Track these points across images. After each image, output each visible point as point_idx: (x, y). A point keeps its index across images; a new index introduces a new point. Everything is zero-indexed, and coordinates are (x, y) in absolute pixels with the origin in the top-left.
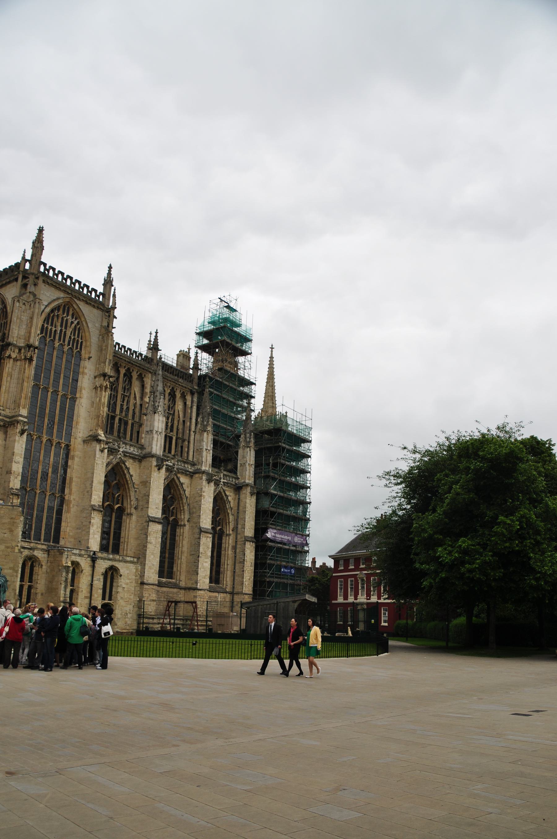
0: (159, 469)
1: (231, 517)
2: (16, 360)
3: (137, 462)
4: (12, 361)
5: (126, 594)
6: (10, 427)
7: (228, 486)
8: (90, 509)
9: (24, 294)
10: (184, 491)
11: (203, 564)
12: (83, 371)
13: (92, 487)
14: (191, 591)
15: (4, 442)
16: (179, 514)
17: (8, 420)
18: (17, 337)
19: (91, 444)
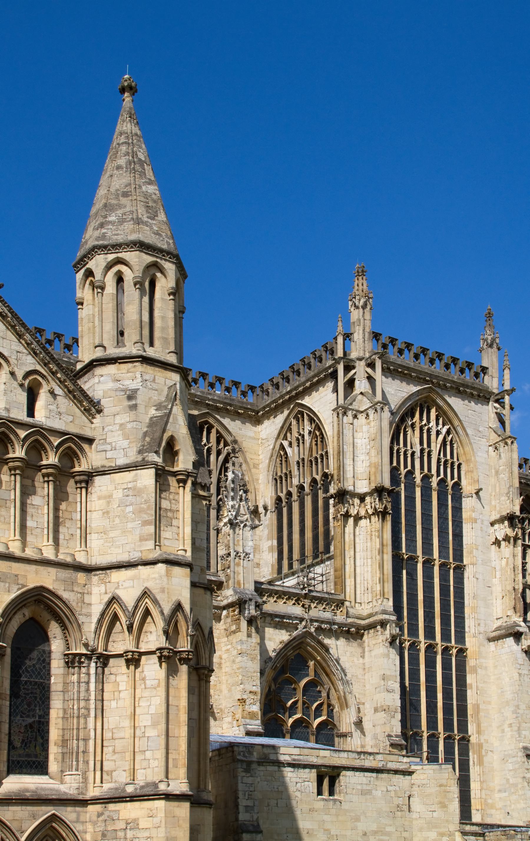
6: (368, 633)
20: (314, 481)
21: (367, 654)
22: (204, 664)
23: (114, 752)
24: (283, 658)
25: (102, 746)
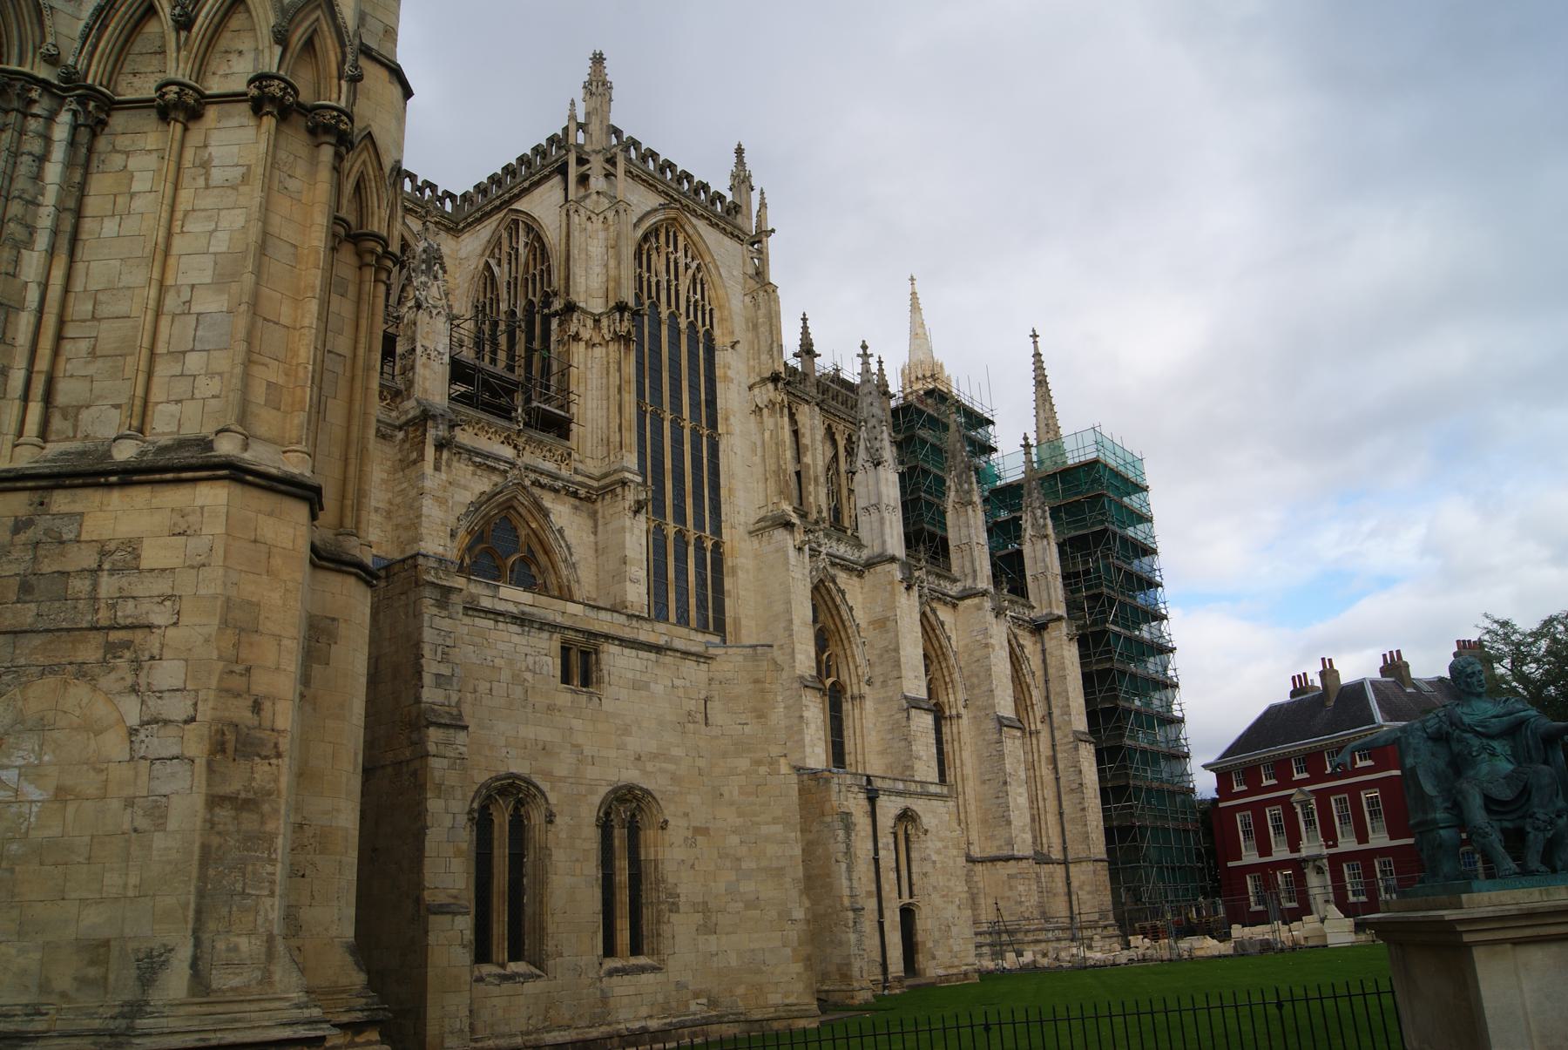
0: (909, 588)
1: (1035, 693)
2: (591, 345)
3: (855, 578)
4: (582, 344)
5: (940, 877)
6: (603, 499)
7: (1020, 625)
8: (796, 685)
9: (586, 196)
10: (949, 638)
11: (1015, 799)
12: (725, 373)
13: (791, 635)
14: (999, 865)
15: (592, 538)
16: (945, 693)
17: (595, 484)
18: (586, 292)
19: (770, 536)
20: (531, 303)
21: (600, 528)
22: (376, 230)
23: (93, 354)
24: (482, 518)
25: (59, 338)
